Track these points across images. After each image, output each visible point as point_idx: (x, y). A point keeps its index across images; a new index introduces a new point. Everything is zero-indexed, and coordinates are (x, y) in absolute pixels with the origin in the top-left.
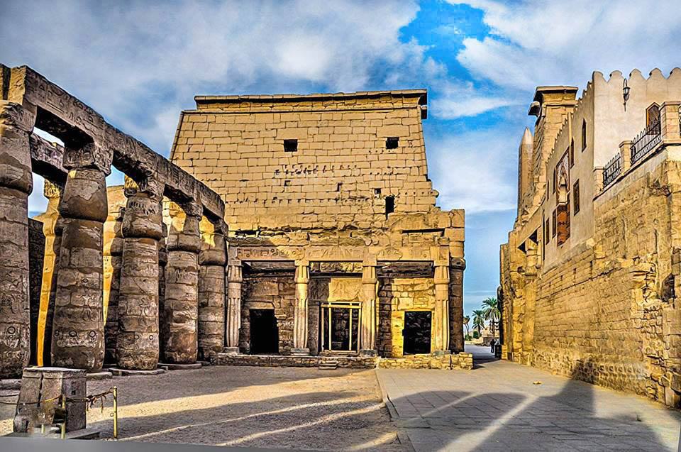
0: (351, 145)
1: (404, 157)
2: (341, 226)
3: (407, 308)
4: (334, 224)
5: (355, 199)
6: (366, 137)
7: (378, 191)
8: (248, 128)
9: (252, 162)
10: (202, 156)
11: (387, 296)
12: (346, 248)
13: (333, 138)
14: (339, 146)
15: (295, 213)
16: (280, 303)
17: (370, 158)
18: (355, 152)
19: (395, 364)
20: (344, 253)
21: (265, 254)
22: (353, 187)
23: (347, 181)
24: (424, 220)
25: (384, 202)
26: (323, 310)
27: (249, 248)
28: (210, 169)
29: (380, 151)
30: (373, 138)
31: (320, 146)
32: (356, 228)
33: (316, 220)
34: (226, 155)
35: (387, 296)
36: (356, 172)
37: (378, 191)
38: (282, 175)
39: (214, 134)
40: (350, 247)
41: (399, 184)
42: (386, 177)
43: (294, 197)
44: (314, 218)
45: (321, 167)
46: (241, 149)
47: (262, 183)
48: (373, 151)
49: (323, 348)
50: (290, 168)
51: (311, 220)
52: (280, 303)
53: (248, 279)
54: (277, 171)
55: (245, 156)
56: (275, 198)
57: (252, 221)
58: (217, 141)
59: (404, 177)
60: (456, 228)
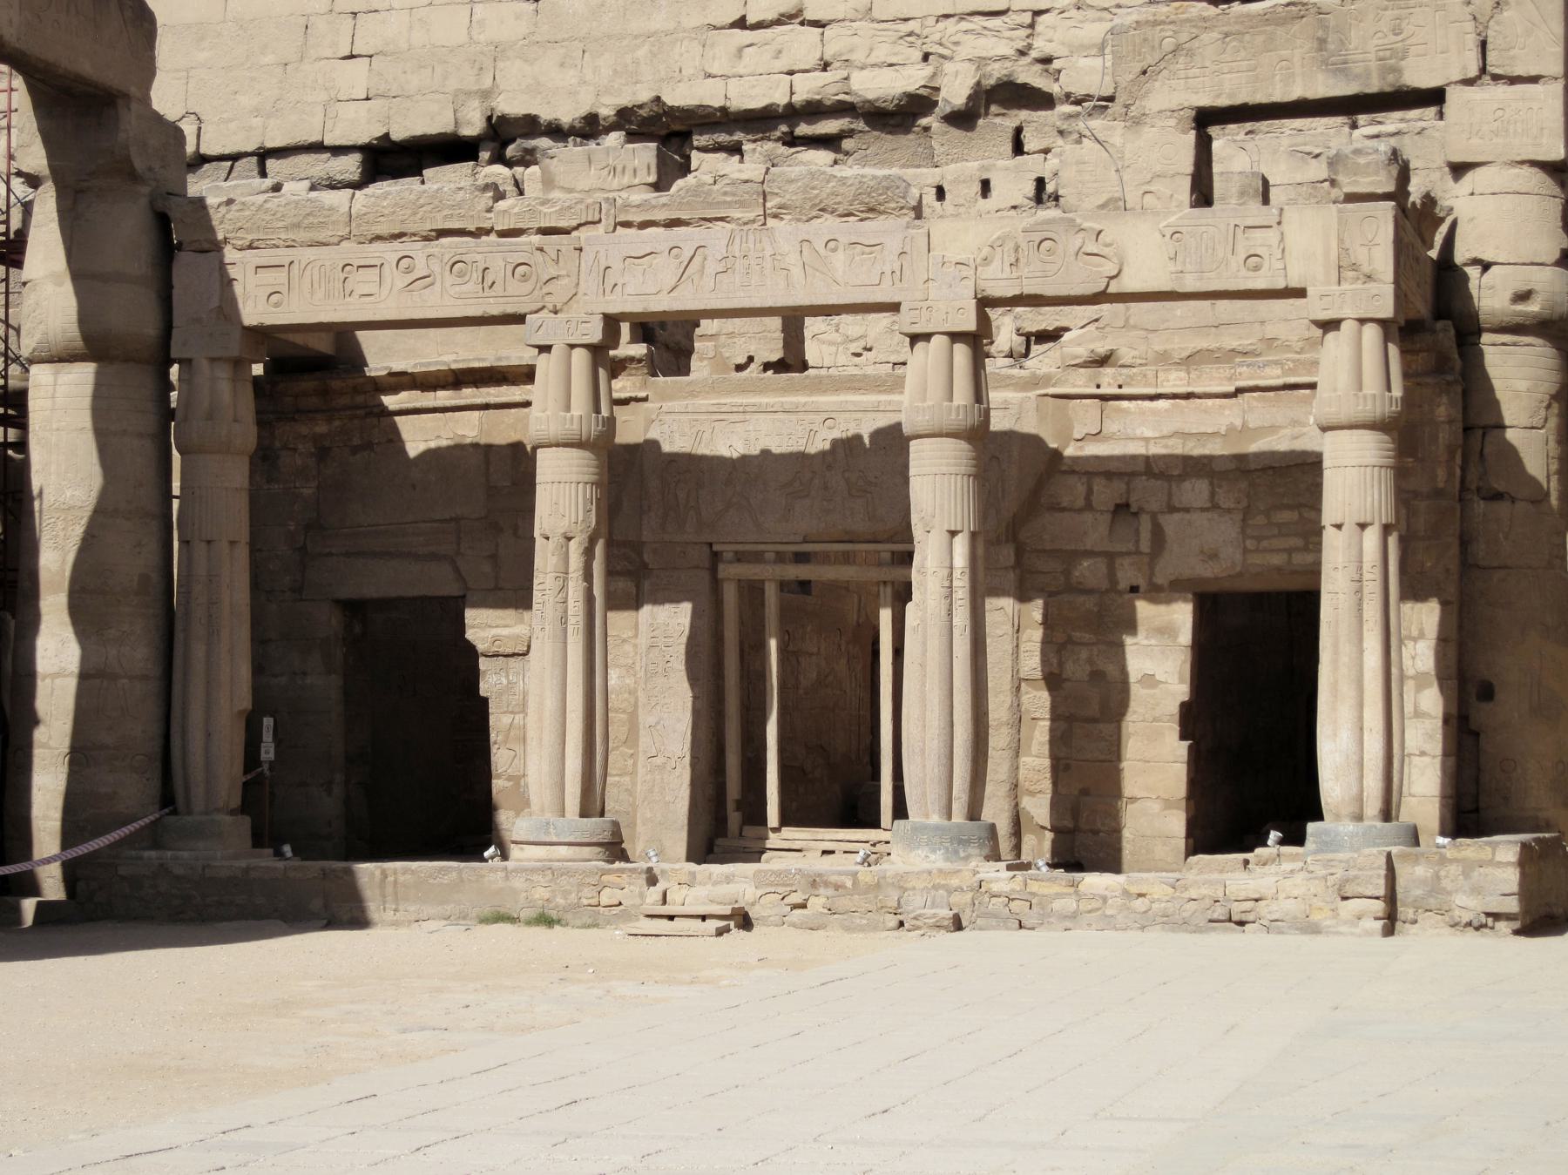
2: (955, 93)
3: (1206, 571)
4: (910, 79)
11: (1088, 506)
12: (806, 230)
15: (694, 20)
16: (494, 558)
19: (1069, 904)
20: (793, 259)
21: (364, 282)
24: (1322, 42)
26: (730, 594)
27: (283, 256)
32: (1044, 101)
33: (812, 60)
35: (1088, 506)
40: (829, 224)
44: (801, 44)
49: (734, 818)
51: (784, 63)
52: (494, 558)
53: (322, 428)
57: (452, 85)
60: (1514, 80)
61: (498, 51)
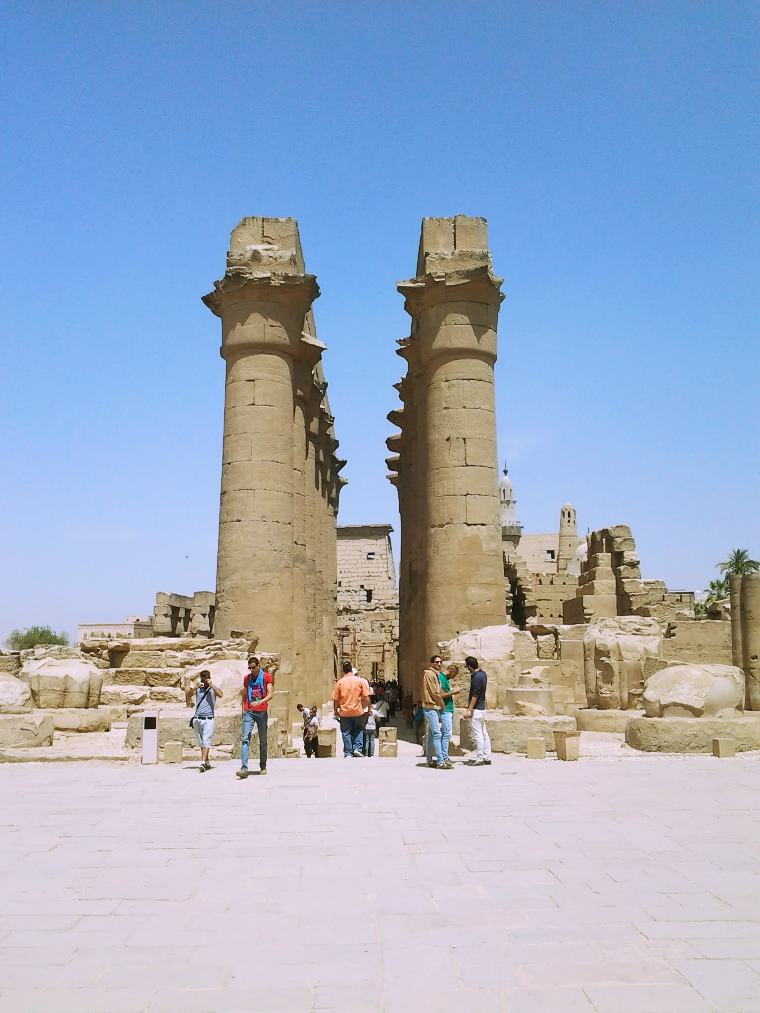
0: (347, 558)
1: (378, 565)
7: (362, 587)
17: (358, 565)
22: (347, 584)
25: (365, 593)
30: (359, 553)
36: (349, 575)
37: (362, 587)
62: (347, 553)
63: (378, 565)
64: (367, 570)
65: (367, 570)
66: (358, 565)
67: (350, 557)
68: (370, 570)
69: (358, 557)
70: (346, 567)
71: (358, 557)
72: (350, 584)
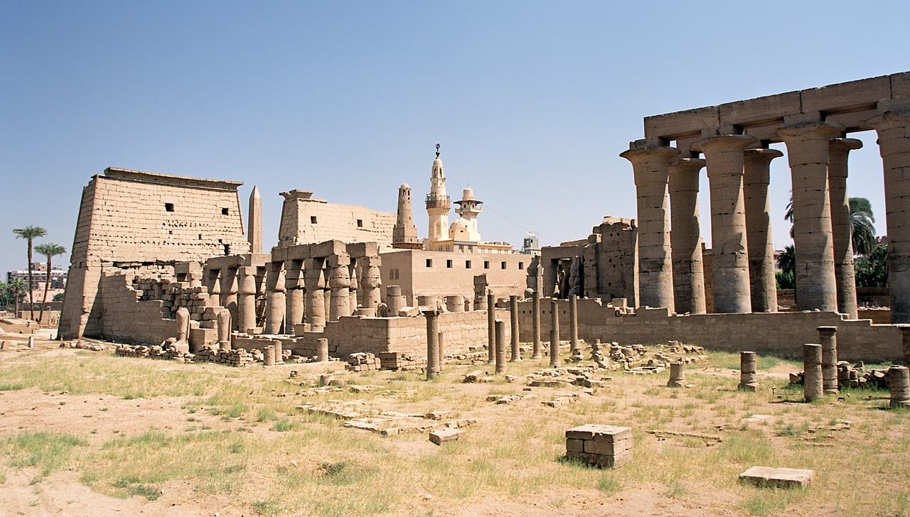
0: (204, 211)
1: (232, 221)
5: (209, 245)
6: (211, 207)
8: (143, 192)
9: (149, 216)
10: (115, 209)
13: (194, 205)
14: (198, 211)
18: (206, 215)
23: (204, 234)
25: (224, 248)
28: (121, 219)
29: (219, 217)
31: (186, 209)
34: (131, 210)
36: (208, 228)
37: (220, 241)
38: (167, 226)
39: (121, 194)
41: (231, 237)
42: (224, 233)
43: (176, 242)
45: (189, 224)
46: (140, 207)
47: (156, 231)
48: (216, 216)
50: (172, 224)
54: (164, 224)
55: (142, 211)
56: (165, 242)
58: (123, 199)
59: (233, 233)
61: (158, 253)
62: (204, 206)
63: (232, 221)
64: (223, 225)
65: (223, 225)
66: (215, 220)
67: (208, 211)
68: (227, 225)
69: (214, 212)
70: (204, 220)
71: (214, 212)
72: (210, 237)
